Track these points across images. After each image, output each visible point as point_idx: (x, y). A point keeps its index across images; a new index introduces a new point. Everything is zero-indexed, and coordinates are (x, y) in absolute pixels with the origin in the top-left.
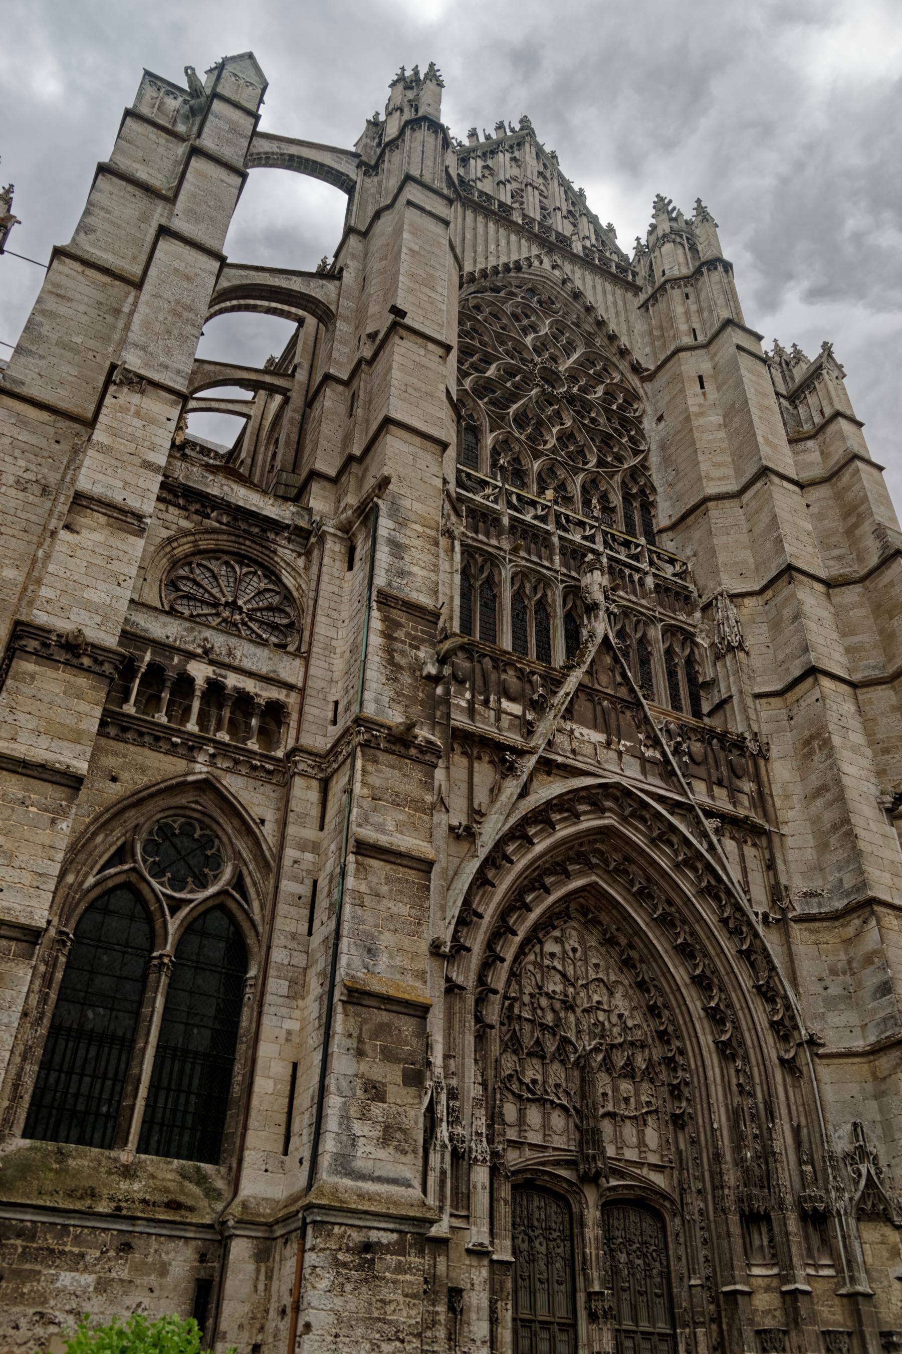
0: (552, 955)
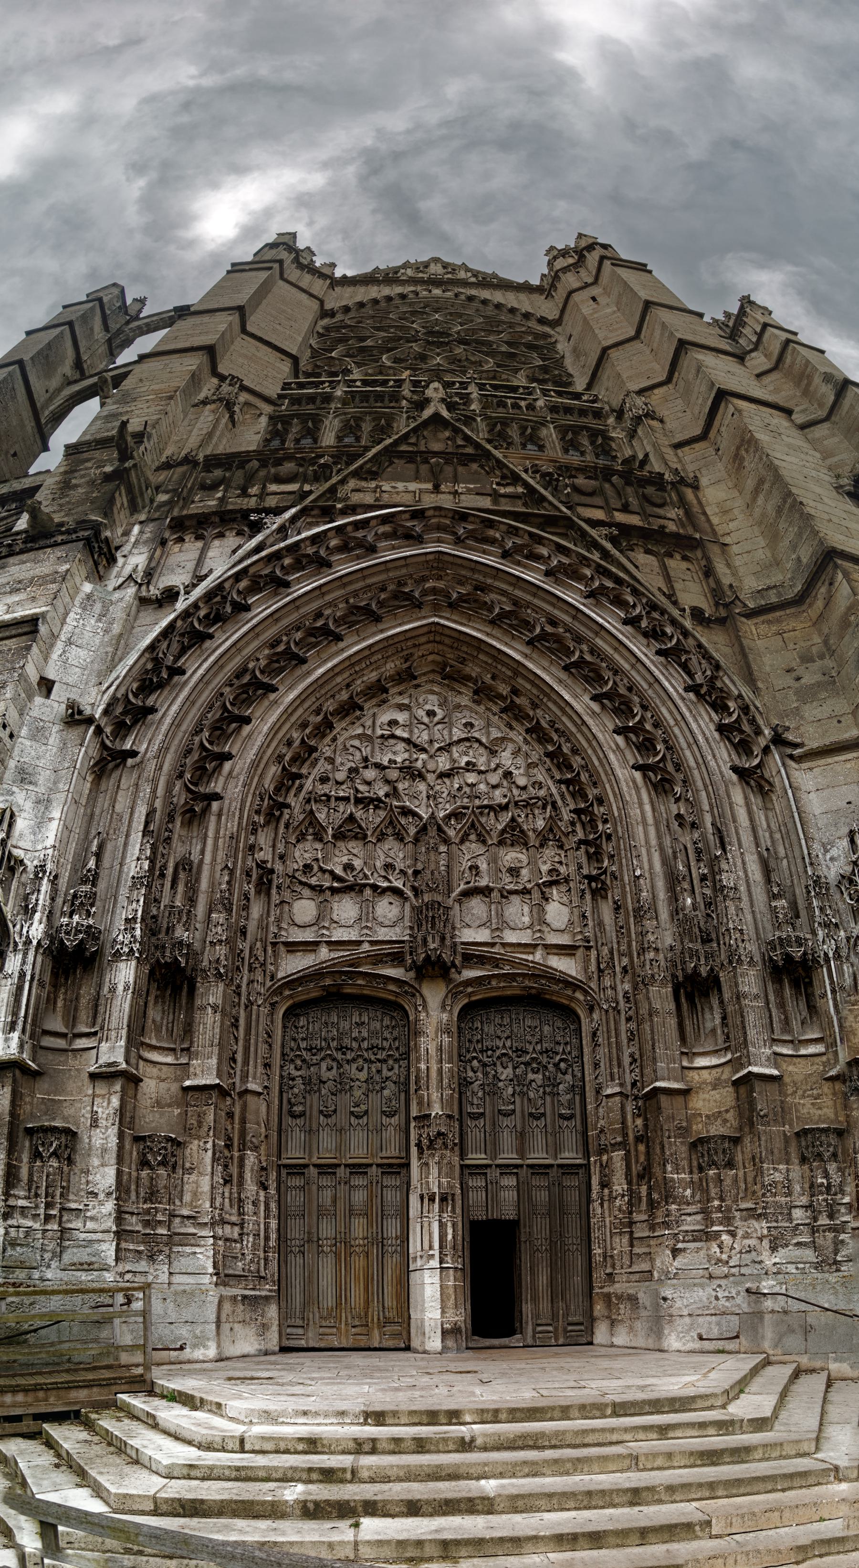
0: (393, 723)
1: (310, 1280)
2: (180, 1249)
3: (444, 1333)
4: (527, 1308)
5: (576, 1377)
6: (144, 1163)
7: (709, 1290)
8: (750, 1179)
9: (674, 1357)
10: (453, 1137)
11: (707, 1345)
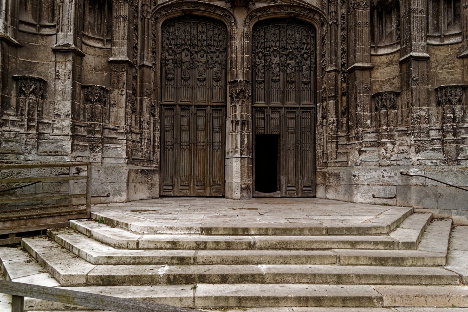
1: (176, 162)
2: (108, 145)
3: (242, 189)
4: (283, 178)
5: (308, 213)
6: (87, 100)
7: (379, 172)
8: (405, 115)
9: (359, 206)
10: (248, 92)
11: (377, 201)
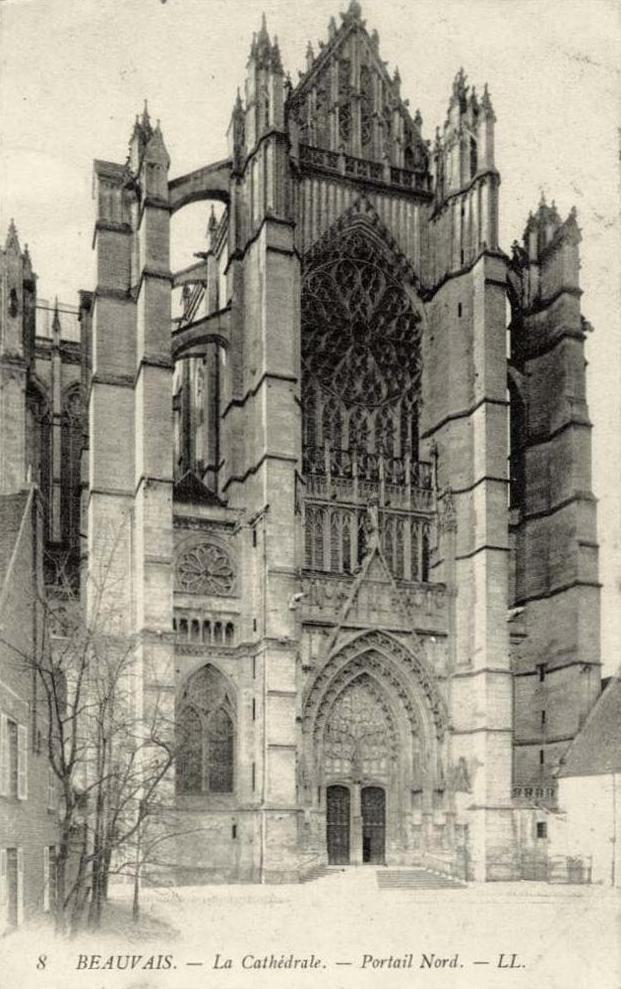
0: (346, 702)
